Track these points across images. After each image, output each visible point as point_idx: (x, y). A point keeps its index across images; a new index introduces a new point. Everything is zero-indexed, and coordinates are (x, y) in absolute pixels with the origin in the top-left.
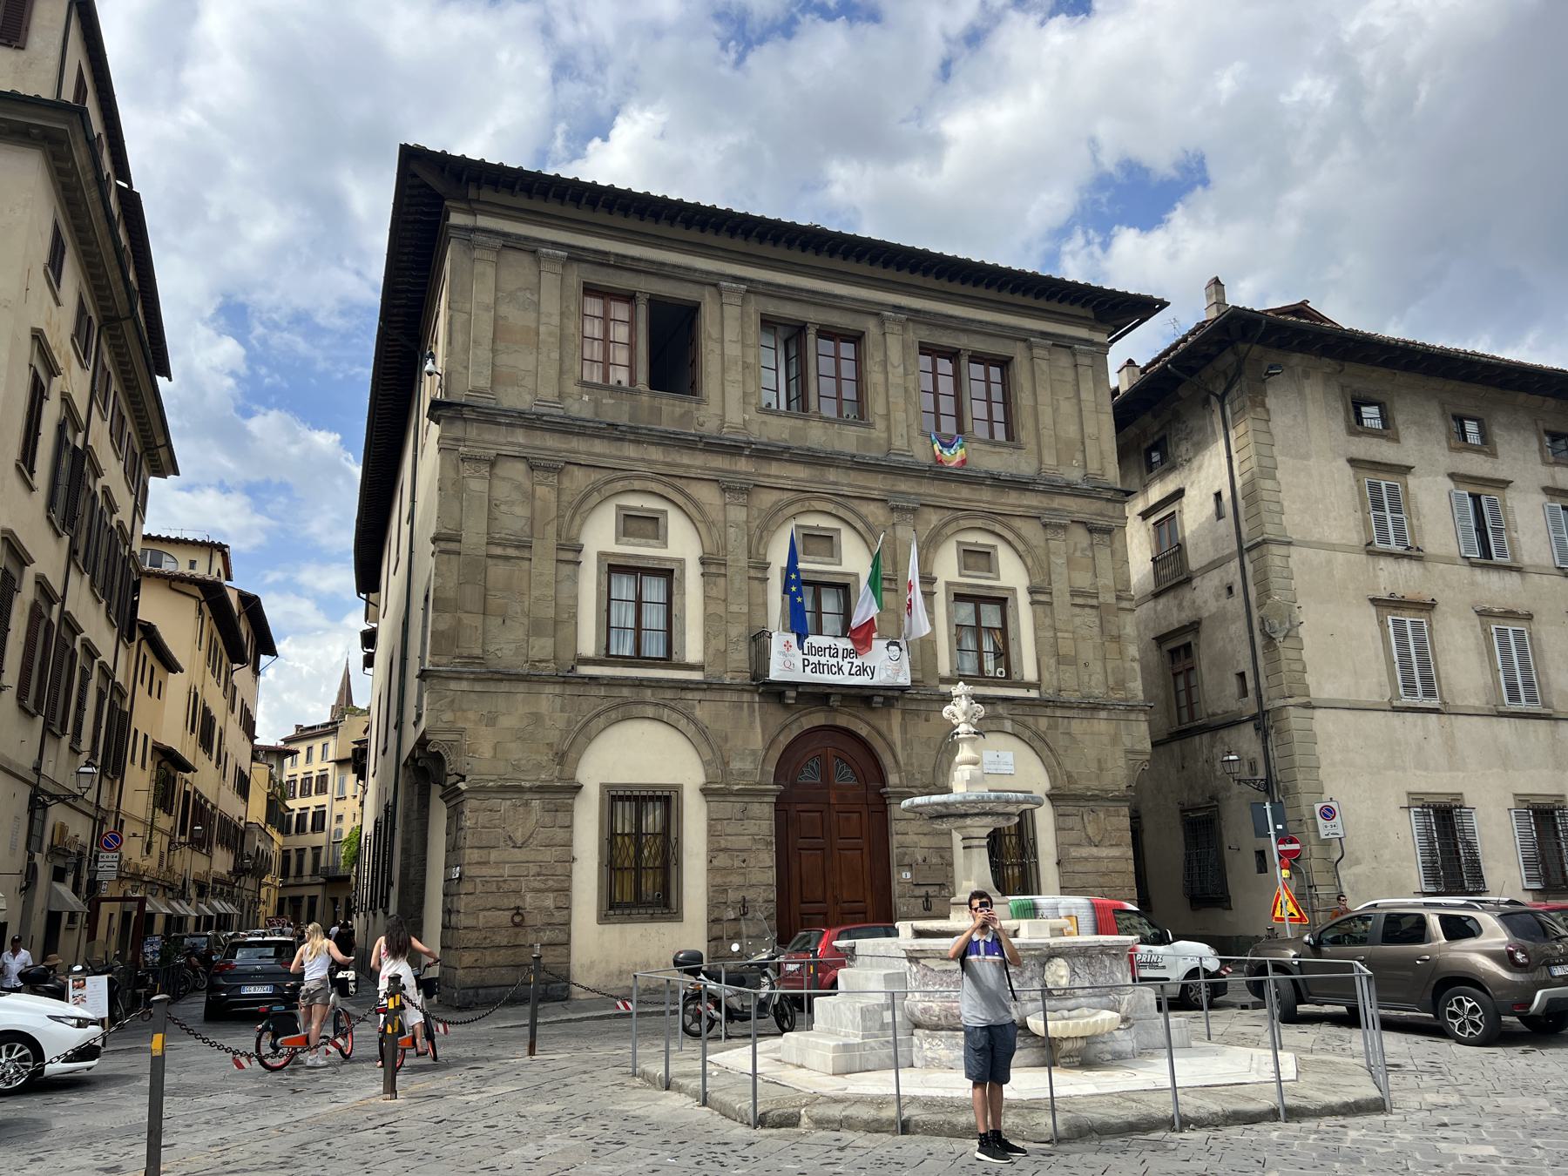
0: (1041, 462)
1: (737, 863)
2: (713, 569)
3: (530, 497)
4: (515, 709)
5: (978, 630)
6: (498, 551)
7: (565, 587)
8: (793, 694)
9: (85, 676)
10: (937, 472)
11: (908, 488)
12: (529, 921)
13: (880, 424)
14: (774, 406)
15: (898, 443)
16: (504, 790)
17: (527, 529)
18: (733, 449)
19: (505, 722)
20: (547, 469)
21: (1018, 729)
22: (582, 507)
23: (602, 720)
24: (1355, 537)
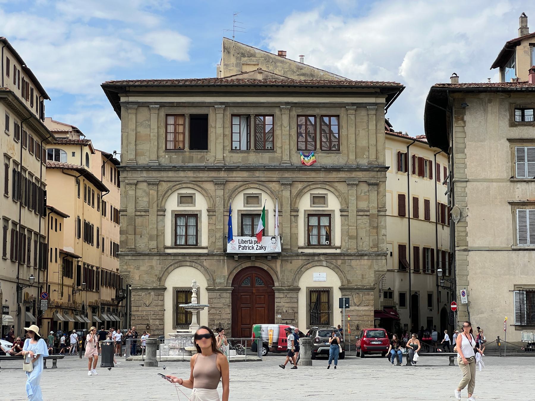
0: (348, 158)
1: (218, 312)
2: (211, 213)
3: (148, 194)
4: (145, 264)
5: (319, 227)
6: (139, 213)
7: (160, 224)
8: (237, 257)
9: (30, 239)
10: (303, 168)
11: (289, 176)
12: (151, 328)
13: (279, 151)
14: (238, 148)
15: (286, 158)
16: (142, 289)
17: (148, 205)
18: (218, 169)
19: (142, 268)
20: (153, 184)
21: (328, 264)
22: (165, 196)
23: (172, 267)
24: (506, 175)
